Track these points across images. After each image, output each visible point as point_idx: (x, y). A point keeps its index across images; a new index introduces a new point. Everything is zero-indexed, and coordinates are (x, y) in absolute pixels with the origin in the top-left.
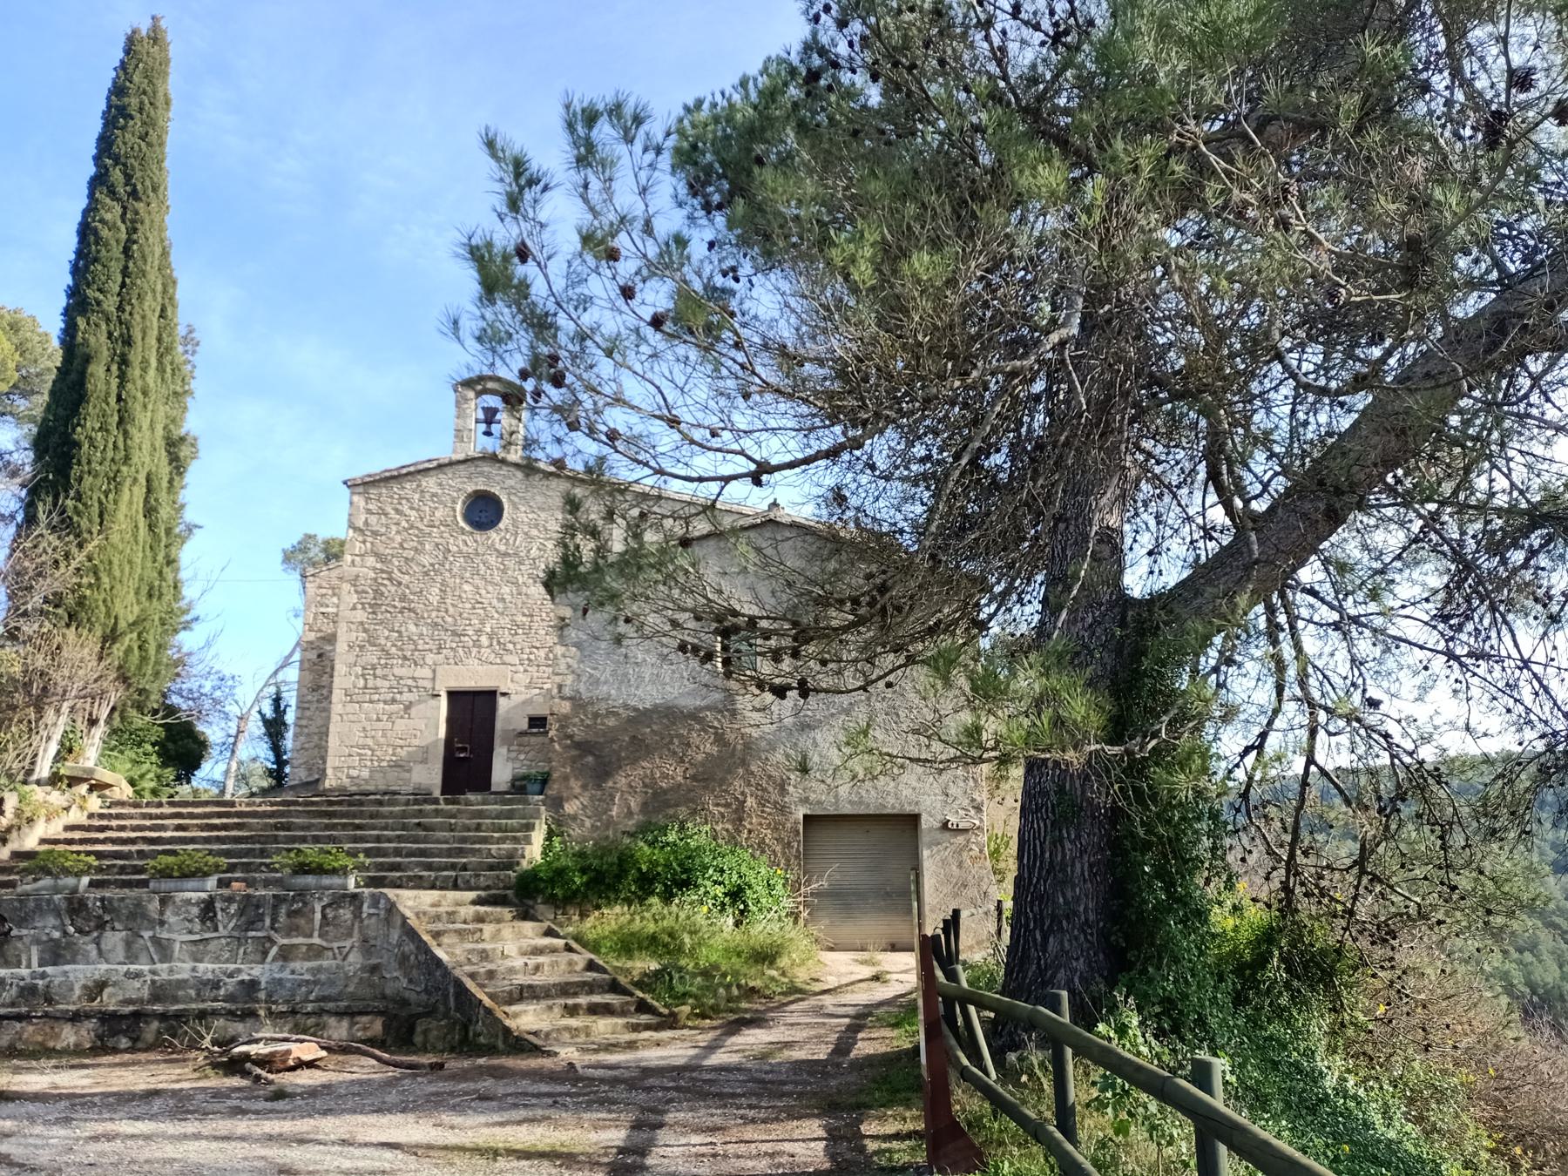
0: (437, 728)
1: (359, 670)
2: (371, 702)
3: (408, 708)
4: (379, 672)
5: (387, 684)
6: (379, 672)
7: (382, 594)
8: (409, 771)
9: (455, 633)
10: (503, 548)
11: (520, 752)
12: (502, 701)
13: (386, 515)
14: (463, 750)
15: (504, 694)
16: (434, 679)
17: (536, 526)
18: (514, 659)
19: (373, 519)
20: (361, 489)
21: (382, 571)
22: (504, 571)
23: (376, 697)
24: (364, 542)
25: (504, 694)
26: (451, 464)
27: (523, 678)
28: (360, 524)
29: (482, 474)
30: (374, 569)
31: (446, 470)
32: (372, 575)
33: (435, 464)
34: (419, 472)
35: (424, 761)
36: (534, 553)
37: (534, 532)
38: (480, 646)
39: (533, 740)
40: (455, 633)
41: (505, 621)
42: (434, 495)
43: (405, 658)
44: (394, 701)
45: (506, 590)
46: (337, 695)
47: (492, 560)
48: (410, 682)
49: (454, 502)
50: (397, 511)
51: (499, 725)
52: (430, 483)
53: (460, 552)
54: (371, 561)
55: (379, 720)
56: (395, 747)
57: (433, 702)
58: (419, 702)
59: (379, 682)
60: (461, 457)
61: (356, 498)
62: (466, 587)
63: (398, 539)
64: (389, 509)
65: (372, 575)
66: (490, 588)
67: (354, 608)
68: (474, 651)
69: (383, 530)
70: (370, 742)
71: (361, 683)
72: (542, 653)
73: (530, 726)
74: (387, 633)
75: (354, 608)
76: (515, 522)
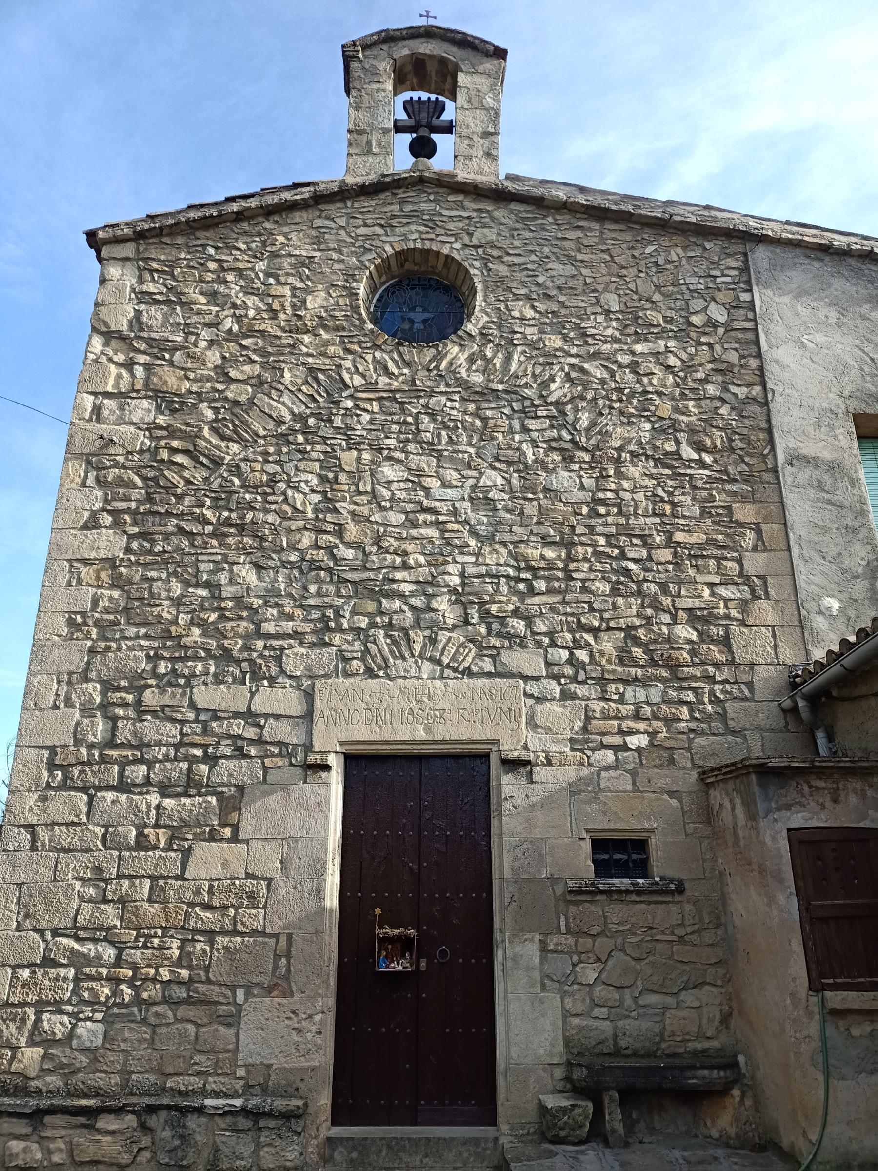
0: (320, 872)
1: (94, 690)
2: (123, 786)
4: (150, 698)
5: (172, 731)
6: (150, 698)
7: (170, 488)
8: (233, 1020)
9: (363, 590)
10: (478, 379)
11: (581, 957)
13: (187, 305)
16: (308, 716)
17: (559, 328)
19: (154, 316)
20: (128, 250)
21: (172, 432)
22: (486, 434)
24: (129, 365)
25: (513, 765)
28: (121, 322)
30: (152, 428)
31: (331, 209)
32: (143, 440)
33: (307, 192)
36: (558, 389)
37: (554, 342)
38: (434, 625)
39: (616, 913)
40: (363, 590)
43: (227, 656)
45: (493, 479)
47: (453, 408)
48: (238, 727)
49: (350, 277)
50: (213, 296)
53: (370, 387)
55: (142, 844)
56: (189, 935)
57: (307, 790)
59: (150, 729)
61: (114, 271)
62: (388, 471)
63: (214, 357)
65: (143, 440)
66: (451, 475)
67: (92, 524)
68: (419, 638)
69: (179, 338)
70: (111, 915)
72: (608, 644)
73: (602, 868)
74: (177, 589)
75: (92, 524)
76: (502, 320)
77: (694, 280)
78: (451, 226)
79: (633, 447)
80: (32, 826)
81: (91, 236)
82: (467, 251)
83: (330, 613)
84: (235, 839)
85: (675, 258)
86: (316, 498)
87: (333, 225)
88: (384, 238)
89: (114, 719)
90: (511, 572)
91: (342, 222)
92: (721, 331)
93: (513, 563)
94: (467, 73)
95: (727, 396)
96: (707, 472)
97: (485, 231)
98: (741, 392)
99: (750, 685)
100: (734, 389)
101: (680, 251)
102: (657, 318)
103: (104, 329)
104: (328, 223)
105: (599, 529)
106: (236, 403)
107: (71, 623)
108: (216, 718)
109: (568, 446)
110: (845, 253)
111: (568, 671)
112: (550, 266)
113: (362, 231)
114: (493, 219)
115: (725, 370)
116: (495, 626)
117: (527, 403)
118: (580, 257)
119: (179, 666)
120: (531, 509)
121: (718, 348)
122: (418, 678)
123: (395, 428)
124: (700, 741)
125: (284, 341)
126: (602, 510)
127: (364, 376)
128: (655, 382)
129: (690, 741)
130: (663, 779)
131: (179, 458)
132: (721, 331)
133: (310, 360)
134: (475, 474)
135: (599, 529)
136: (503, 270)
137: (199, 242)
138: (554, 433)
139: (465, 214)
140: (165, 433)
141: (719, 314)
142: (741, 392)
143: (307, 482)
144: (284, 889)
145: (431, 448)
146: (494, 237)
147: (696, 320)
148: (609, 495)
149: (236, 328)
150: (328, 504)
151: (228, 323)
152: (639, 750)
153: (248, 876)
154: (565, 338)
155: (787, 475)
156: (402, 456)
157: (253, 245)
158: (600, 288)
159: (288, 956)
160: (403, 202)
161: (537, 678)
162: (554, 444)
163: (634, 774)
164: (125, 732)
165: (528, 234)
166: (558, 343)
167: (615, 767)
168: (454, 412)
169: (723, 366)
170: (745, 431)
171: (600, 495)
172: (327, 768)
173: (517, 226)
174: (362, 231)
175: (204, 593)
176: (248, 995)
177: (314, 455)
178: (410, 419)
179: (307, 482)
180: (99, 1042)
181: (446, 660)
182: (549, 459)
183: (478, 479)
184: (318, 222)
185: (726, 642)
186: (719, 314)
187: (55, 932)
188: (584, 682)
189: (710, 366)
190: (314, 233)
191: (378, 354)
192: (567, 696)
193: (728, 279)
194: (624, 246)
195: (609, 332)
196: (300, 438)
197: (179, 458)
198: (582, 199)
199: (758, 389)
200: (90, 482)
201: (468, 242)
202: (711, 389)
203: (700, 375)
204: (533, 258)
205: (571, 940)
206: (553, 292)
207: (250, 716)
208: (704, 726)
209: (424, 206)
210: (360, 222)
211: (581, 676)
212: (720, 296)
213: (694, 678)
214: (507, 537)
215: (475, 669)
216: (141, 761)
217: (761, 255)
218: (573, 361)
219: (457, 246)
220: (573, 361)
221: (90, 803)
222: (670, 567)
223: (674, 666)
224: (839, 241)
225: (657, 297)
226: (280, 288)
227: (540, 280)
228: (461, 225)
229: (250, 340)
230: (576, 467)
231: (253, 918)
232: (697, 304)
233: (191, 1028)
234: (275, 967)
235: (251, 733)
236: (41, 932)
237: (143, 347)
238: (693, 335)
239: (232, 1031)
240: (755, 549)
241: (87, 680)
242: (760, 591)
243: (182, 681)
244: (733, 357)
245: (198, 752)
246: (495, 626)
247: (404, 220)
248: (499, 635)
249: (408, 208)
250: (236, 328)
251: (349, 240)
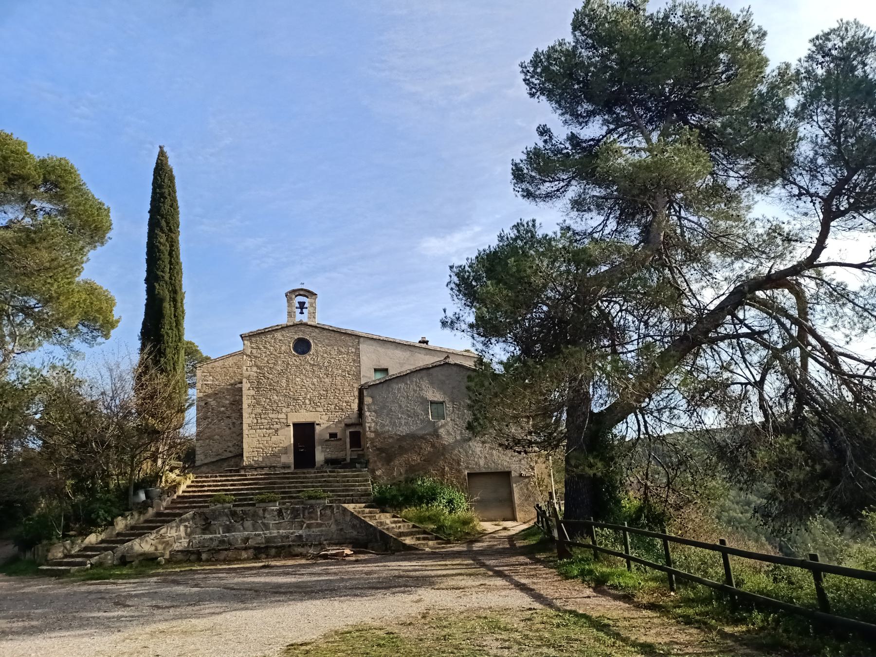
2: (260, 429)
3: (277, 431)
5: (266, 421)
8: (280, 457)
9: (294, 399)
10: (312, 362)
11: (327, 448)
12: (317, 427)
13: (260, 349)
14: (302, 448)
15: (318, 424)
17: (326, 353)
18: (321, 409)
19: (254, 351)
20: (248, 338)
21: (260, 373)
22: (314, 372)
23: (262, 427)
24: (251, 361)
25: (318, 424)
26: (287, 327)
27: (325, 417)
29: (301, 331)
30: (257, 372)
31: (285, 329)
33: (280, 327)
34: (273, 330)
35: (286, 453)
36: (326, 364)
37: (325, 355)
39: (332, 443)
40: (294, 399)
41: (316, 393)
42: (280, 340)
43: (273, 410)
44: (270, 428)
45: (315, 380)
46: (245, 427)
47: (308, 368)
48: (276, 420)
50: (265, 347)
51: (317, 437)
52: (278, 335)
53: (294, 364)
54: (255, 369)
55: (264, 436)
56: (273, 448)
57: (287, 428)
58: (281, 428)
59: (263, 421)
60: (291, 324)
61: (246, 342)
62: (298, 379)
64: (261, 346)
66: (308, 380)
67: (249, 389)
68: (303, 406)
70: (261, 445)
71: (255, 421)
72: (333, 407)
75: (249, 389)
76: (317, 351)
81: (241, 336)
102: (343, 350)
110: (375, 339)
120: (321, 385)
130: (339, 425)
144: (285, 441)
145: (305, 375)
150: (288, 385)
164: (259, 421)
185: (350, 406)
186: (353, 350)
198: (331, 328)
207: (278, 418)
217: (362, 339)
223: (342, 409)
224: (375, 337)
231: (281, 445)
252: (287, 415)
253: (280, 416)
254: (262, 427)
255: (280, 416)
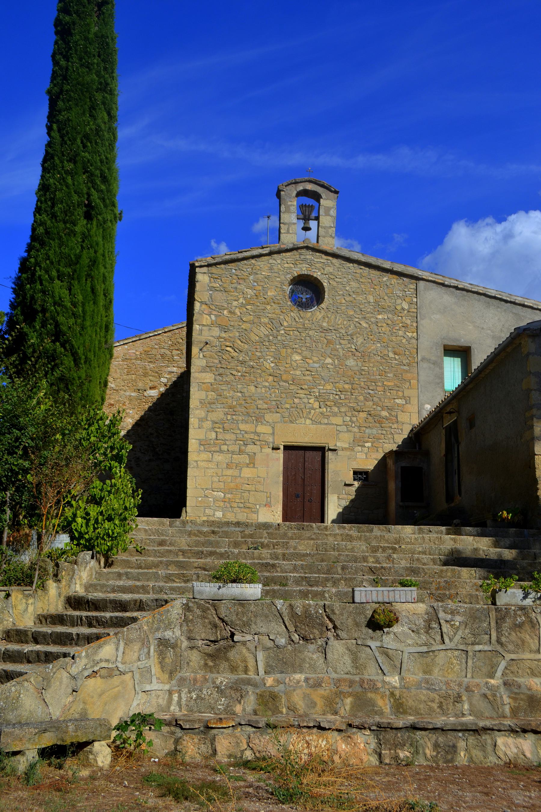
8: (257, 512)
16: (273, 434)
20: (205, 269)
23: (225, 448)
29: (305, 260)
31: (275, 256)
35: (268, 505)
44: (241, 452)
71: (213, 435)
77: (398, 292)
78: (317, 265)
79: (375, 352)
80: (197, 461)
82: (322, 276)
83: (278, 402)
84: (254, 467)
85: (393, 283)
86: (272, 365)
87: (276, 263)
88: (294, 269)
89: (216, 432)
90: (335, 393)
91: (279, 261)
92: (406, 312)
93: (334, 389)
94: (324, 199)
95: (405, 336)
96: (396, 362)
97: (329, 268)
98: (410, 335)
99: (402, 430)
100: (407, 333)
101: (395, 280)
103: (200, 301)
104: (274, 262)
105: (362, 380)
106: (246, 330)
107: (201, 403)
108: (246, 433)
109: (354, 350)
111: (350, 423)
112: (351, 283)
113: (286, 265)
114: (331, 263)
115: (405, 326)
116: (328, 409)
117: (341, 334)
118: (361, 280)
119: (234, 417)
120: (341, 371)
121: (404, 318)
122: (305, 424)
123: (298, 341)
124: (386, 445)
125: (260, 308)
126: (363, 373)
127: (287, 322)
128: (383, 329)
129: (383, 445)
131: (228, 349)
132: (406, 312)
133: (270, 315)
134: (323, 358)
135: (362, 380)
136: (335, 284)
137: (229, 267)
138: (349, 346)
139: (322, 261)
140: (223, 340)
141: (406, 306)
142: (410, 335)
143: (269, 359)
146: (332, 271)
147: (399, 308)
148: (366, 368)
149: (244, 302)
151: (241, 300)
152: (368, 448)
153: (258, 477)
154: (355, 311)
155: (421, 364)
156: (300, 351)
157: (248, 270)
158: (367, 293)
159: (270, 498)
160: (300, 254)
161: (340, 425)
162: (349, 349)
163: (366, 454)
165: (344, 270)
166: (352, 313)
167: (361, 452)
168: (317, 337)
169: (405, 325)
170: (409, 349)
171: (363, 368)
172: (279, 449)
173: (340, 266)
174: (286, 265)
175: (239, 394)
176: (260, 507)
177: (272, 350)
178: (303, 338)
179: (269, 359)
180: (221, 516)
181: (313, 419)
182: (347, 355)
183: (324, 361)
184: (271, 261)
186: (406, 306)
187: (207, 489)
188: (354, 427)
189: (401, 325)
190: (269, 265)
191: (292, 314)
192: (349, 431)
193: (410, 293)
194: (377, 277)
195: (369, 310)
196: (267, 344)
197: (228, 349)
199: (415, 334)
200: (201, 356)
201: (323, 272)
202: (401, 333)
203: (397, 328)
204: (345, 280)
205: (346, 496)
206: (351, 294)
207: (255, 433)
208: (388, 441)
209: (308, 257)
210: (285, 262)
211: (353, 425)
212: (407, 299)
213: (386, 427)
214: (333, 380)
215: (322, 422)
216: (226, 444)
217: (421, 284)
218: (357, 320)
219: (319, 274)
220: (357, 320)
221: (212, 456)
222: (382, 393)
225: (386, 298)
226: (258, 287)
227: (347, 288)
228: (321, 265)
229: (249, 307)
230: (356, 358)
232: (399, 301)
233: (245, 514)
234: (267, 500)
235: (256, 438)
236: (203, 489)
237: (214, 308)
238: (397, 313)
239: (256, 515)
240: (408, 388)
241: (207, 420)
242: (408, 402)
243: (235, 422)
244: (409, 322)
245: (241, 442)
246: (328, 409)
247: (301, 262)
248: (330, 412)
249: (302, 257)
250: (244, 302)
251: (282, 269)
252: (273, 428)
253: (261, 429)
254: (225, 448)
255: (261, 429)
